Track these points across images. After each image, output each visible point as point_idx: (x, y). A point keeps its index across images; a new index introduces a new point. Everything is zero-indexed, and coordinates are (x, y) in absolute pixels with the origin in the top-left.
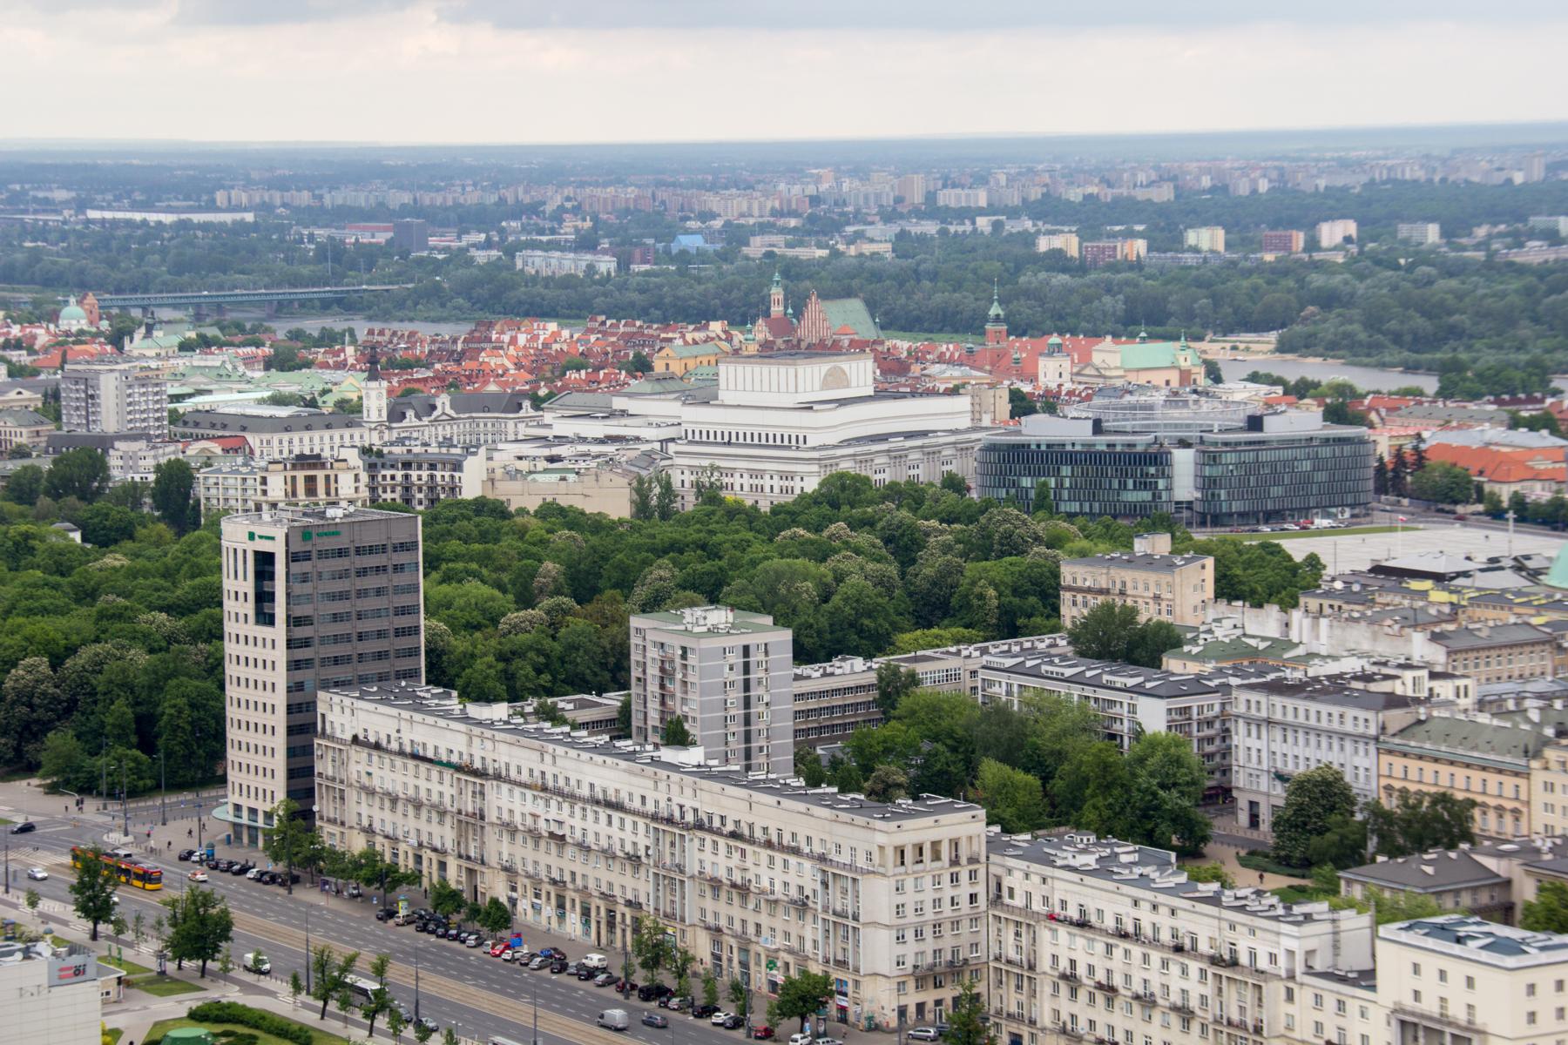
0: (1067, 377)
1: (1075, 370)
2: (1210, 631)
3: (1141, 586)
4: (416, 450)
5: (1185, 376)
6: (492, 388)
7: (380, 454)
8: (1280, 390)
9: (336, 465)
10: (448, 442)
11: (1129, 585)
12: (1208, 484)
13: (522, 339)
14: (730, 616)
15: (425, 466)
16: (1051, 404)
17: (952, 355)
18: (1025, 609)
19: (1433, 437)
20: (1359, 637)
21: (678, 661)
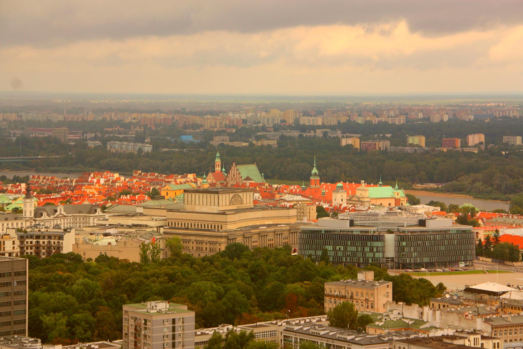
0: (345, 201)
1: (348, 198)
2: (388, 316)
3: (360, 295)
4: (43, 230)
5: (397, 201)
6: (86, 203)
7: (25, 232)
8: (439, 209)
9: (4, 237)
10: (57, 226)
11: (355, 294)
12: (399, 249)
13: (102, 181)
14: (168, 305)
15: (46, 237)
16: (336, 212)
17: (296, 190)
18: (313, 303)
19: (504, 231)
20: (454, 320)
21: (143, 326)
